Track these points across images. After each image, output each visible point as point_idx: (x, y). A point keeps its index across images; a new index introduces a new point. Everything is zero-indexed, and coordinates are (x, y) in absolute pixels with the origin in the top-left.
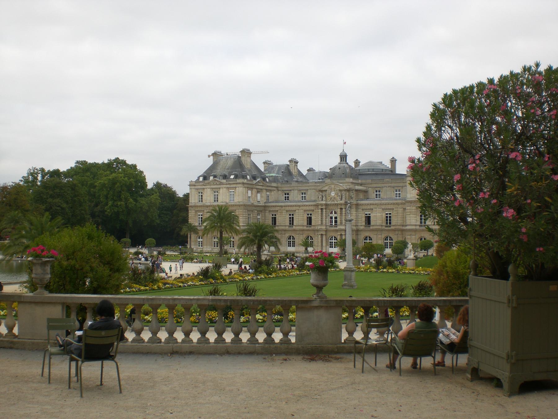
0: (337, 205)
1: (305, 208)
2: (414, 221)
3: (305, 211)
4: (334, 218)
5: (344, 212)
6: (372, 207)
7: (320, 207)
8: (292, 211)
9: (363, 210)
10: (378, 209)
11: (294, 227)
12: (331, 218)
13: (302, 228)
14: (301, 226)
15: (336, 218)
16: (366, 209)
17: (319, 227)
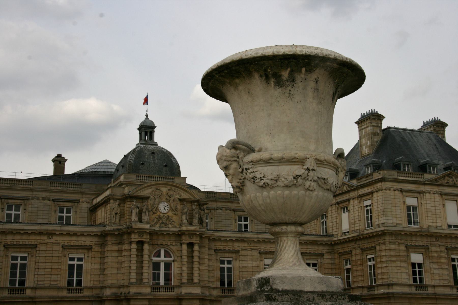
0: (179, 235)
1: (66, 240)
2: (404, 275)
3: (64, 247)
4: (162, 266)
5: (196, 254)
6: (237, 246)
7: (135, 237)
8: (24, 246)
9: (216, 251)
10: (249, 253)
11: (29, 292)
12: (156, 266)
13: (54, 293)
14: (50, 288)
15: (168, 266)
16: (224, 251)
17: (133, 290)
